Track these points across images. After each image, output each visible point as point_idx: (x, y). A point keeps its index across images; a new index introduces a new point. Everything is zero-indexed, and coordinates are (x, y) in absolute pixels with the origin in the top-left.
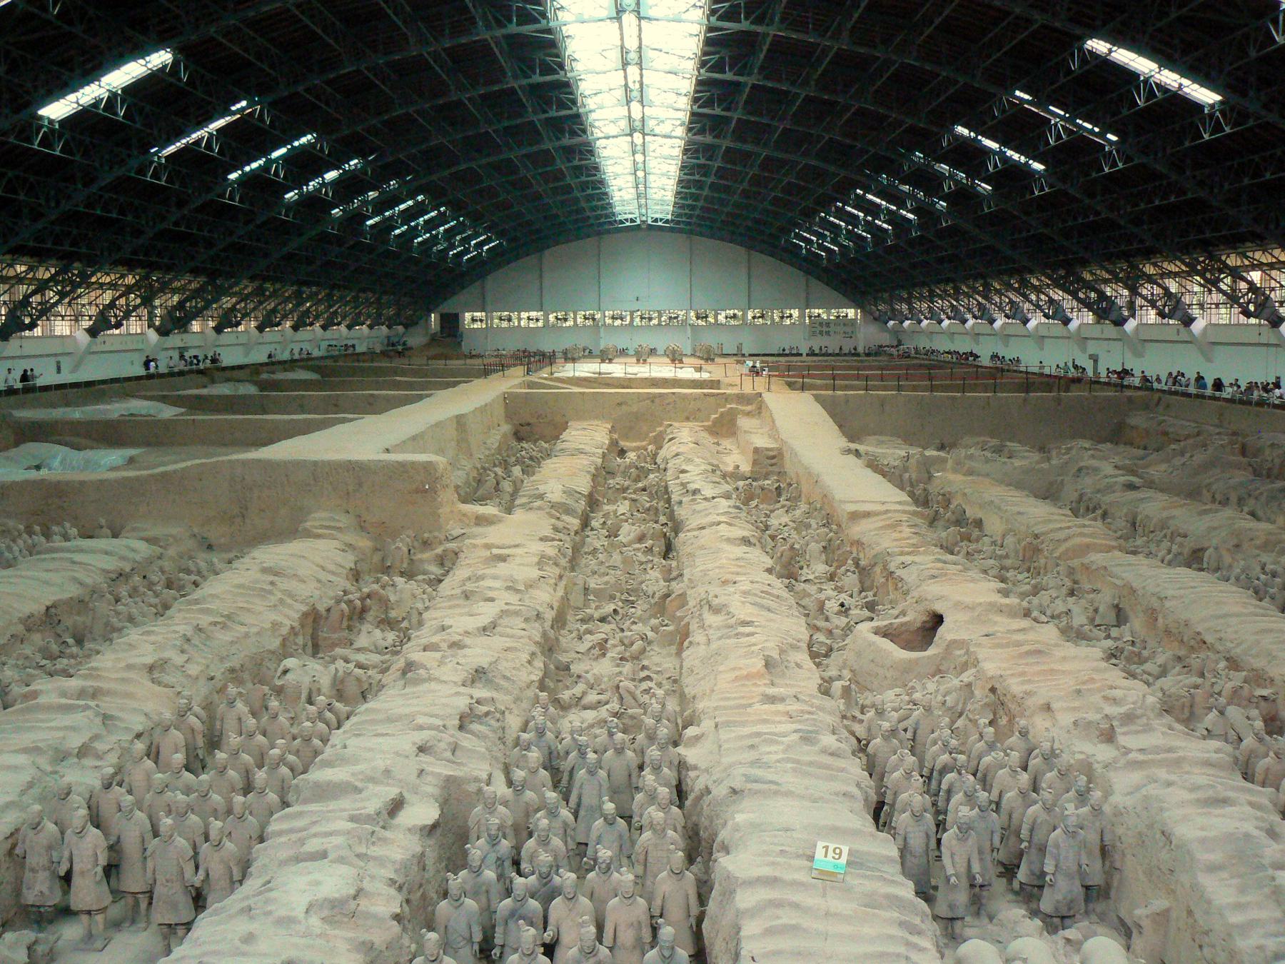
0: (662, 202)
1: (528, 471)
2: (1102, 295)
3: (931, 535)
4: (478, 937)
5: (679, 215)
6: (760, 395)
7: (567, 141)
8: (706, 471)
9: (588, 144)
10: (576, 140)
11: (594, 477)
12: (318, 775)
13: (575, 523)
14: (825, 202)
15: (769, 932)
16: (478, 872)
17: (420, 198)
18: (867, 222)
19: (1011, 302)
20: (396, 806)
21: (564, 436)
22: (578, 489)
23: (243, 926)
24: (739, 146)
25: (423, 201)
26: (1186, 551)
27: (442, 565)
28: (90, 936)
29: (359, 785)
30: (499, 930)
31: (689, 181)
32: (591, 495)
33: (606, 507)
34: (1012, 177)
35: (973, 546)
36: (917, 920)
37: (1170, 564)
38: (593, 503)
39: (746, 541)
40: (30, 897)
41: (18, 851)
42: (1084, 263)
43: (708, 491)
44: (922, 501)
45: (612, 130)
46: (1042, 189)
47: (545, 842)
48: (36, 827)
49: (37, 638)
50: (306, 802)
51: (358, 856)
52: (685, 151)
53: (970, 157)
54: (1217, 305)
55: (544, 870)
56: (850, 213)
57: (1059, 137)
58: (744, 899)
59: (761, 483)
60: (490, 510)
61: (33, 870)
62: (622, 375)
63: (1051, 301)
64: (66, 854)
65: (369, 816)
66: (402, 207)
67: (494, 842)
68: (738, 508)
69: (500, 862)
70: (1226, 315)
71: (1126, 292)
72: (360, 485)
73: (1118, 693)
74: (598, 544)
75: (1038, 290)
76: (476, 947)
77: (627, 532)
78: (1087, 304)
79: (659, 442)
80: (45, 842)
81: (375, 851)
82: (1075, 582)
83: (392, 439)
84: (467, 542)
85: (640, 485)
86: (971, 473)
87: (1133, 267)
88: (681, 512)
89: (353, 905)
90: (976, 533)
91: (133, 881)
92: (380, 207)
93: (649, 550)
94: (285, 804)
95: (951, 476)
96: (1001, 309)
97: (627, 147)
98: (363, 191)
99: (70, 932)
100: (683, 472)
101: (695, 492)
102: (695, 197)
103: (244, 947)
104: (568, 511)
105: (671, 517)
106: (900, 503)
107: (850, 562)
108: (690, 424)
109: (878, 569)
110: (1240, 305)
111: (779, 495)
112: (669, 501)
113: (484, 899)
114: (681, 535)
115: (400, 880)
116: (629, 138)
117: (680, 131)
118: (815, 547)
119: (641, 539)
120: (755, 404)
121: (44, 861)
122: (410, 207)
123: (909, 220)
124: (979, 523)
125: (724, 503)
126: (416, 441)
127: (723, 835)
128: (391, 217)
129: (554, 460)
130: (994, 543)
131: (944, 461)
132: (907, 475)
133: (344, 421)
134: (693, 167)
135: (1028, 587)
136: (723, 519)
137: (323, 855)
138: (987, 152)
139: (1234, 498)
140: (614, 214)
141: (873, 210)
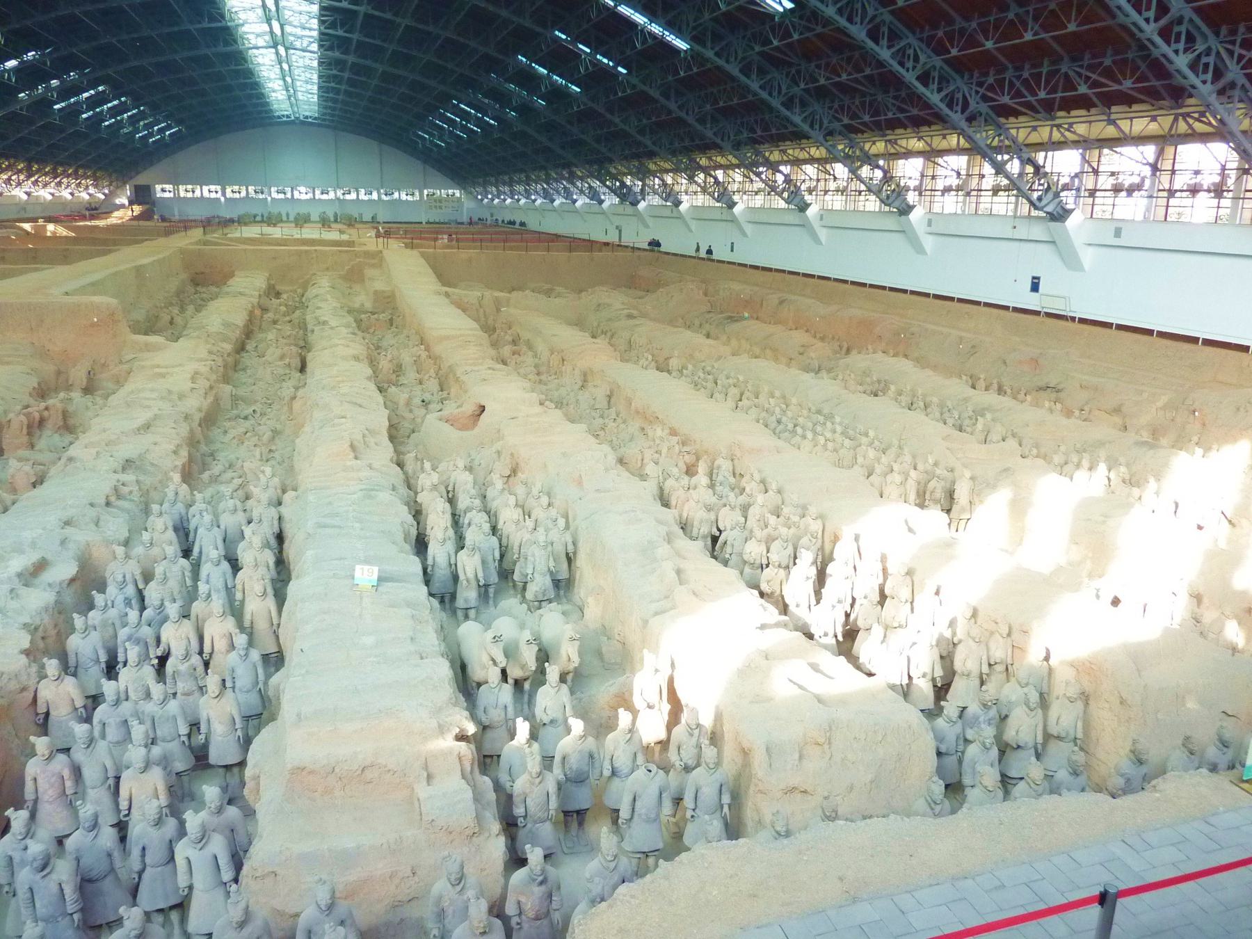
0: (308, 103)
1: (198, 309)
3: (493, 352)
5: (324, 114)
6: (381, 252)
7: (222, 49)
8: (335, 308)
9: (241, 52)
10: (229, 49)
11: (251, 313)
13: (228, 347)
14: (432, 109)
17: (101, 88)
18: (478, 118)
21: (230, 282)
22: (236, 322)
24: (361, 61)
25: (103, 92)
26: (661, 360)
31: (328, 88)
32: (246, 326)
33: (261, 335)
34: (557, 95)
35: (521, 359)
38: (248, 333)
39: (356, 358)
42: (611, 161)
44: (489, 329)
45: (261, 42)
46: (579, 107)
52: (320, 64)
53: (527, 79)
56: (449, 117)
57: (587, 68)
59: (376, 316)
62: (280, 236)
66: (86, 95)
68: (354, 334)
70: (701, 200)
77: (272, 353)
78: (613, 190)
82: (585, 381)
83: (70, 287)
84: (137, 364)
85: (288, 318)
87: (642, 164)
88: (312, 338)
90: (524, 349)
92: (65, 93)
93: (289, 365)
95: (512, 311)
97: (274, 57)
98: (46, 78)
100: (319, 308)
101: (325, 323)
102: (335, 101)
106: (471, 329)
107: (432, 370)
108: (330, 273)
109: (451, 376)
110: (709, 194)
111: (392, 325)
116: (273, 50)
117: (315, 47)
119: (282, 358)
120: (376, 259)
122: (92, 96)
123: (491, 125)
125: (344, 330)
126: (95, 288)
128: (76, 103)
129: (220, 300)
133: (36, 270)
134: (329, 77)
138: (540, 77)
139: (697, 322)
140: (271, 110)
141: (465, 116)
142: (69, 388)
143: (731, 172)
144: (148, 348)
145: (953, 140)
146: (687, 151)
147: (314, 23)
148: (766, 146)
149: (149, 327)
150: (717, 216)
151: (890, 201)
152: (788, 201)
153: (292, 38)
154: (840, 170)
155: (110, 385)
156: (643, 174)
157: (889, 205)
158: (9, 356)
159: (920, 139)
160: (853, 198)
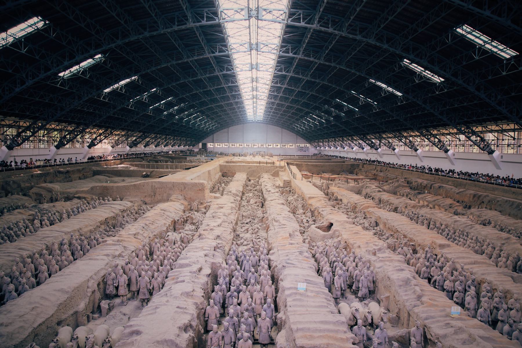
2: (372, 142)
4: (222, 302)
12: (180, 262)
13: (239, 199)
15: (294, 300)
16: (221, 286)
19: (349, 143)
20: (200, 270)
23: (165, 299)
26: (393, 208)
27: (206, 209)
28: (122, 302)
29: (191, 264)
30: (227, 300)
32: (243, 191)
33: (247, 195)
34: (350, 112)
35: (340, 206)
36: (329, 298)
37: (389, 211)
38: (243, 194)
40: (108, 292)
41: (105, 280)
42: (368, 134)
43: (273, 191)
44: (327, 194)
47: (237, 278)
48: (110, 274)
49: (103, 226)
50: (177, 268)
51: (192, 281)
53: (339, 107)
54: (401, 146)
55: (238, 285)
57: (362, 103)
58: (287, 292)
60: (218, 195)
61: (109, 285)
63: (359, 143)
64: (117, 281)
65: (194, 272)
67: (225, 278)
69: (226, 283)
71: (379, 142)
72: (185, 188)
73: (377, 243)
74: (245, 204)
75: (356, 140)
76: (221, 304)
77: (252, 201)
79: (259, 178)
80: (112, 278)
81: (196, 280)
86: (339, 187)
88: (266, 196)
89: (192, 293)
90: (340, 203)
91: (134, 288)
93: (258, 206)
94: (172, 269)
96: (346, 145)
99: (117, 301)
100: (266, 186)
103: (167, 303)
104: (237, 196)
105: (263, 197)
111: (290, 192)
112: (262, 193)
113: (223, 292)
114: (266, 202)
115: (203, 287)
118: (300, 206)
119: (256, 203)
121: (112, 283)
124: (341, 200)
127: (281, 277)
130: (345, 205)
131: (332, 184)
132: (323, 188)
135: (353, 217)
136: (277, 198)
137: (184, 281)
139: (405, 195)
142: (191, 210)
143: (416, 138)
144: (215, 198)
145: (512, 126)
146: (399, 131)
147: (266, 91)
148: (431, 128)
149: (213, 190)
150: (410, 154)
151: (484, 149)
152: (440, 149)
153: (259, 96)
154: (462, 137)
155: (204, 210)
156: (380, 139)
157: (484, 150)
158: (175, 199)
159: (497, 126)
160: (467, 148)
